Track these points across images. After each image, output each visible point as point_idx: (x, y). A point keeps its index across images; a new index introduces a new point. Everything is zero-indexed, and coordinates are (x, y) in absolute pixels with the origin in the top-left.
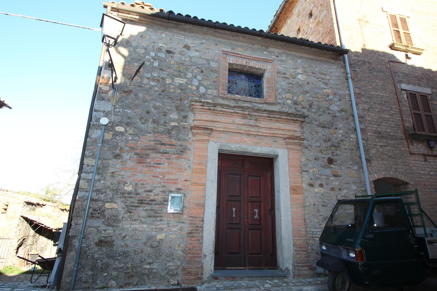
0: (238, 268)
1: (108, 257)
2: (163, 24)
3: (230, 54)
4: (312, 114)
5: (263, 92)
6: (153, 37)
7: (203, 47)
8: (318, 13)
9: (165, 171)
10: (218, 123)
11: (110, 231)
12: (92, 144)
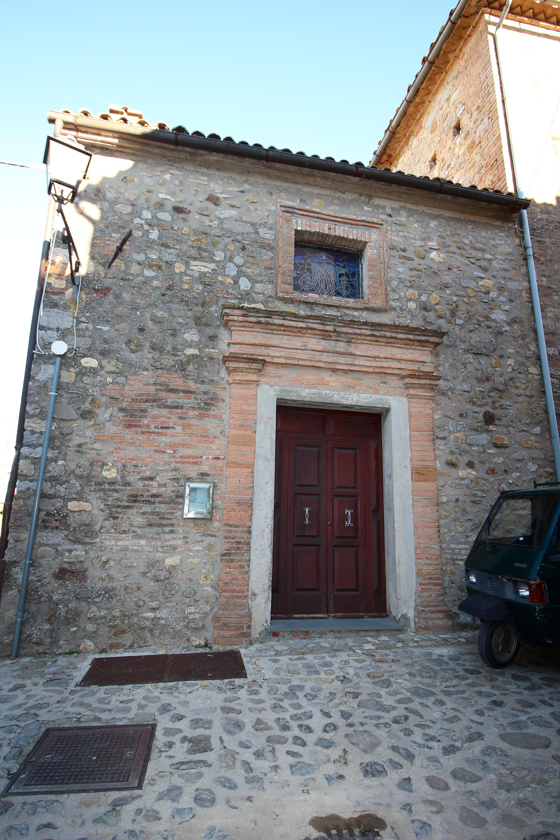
0: (315, 615)
1: (77, 598)
2: (167, 153)
3: (298, 212)
4: (457, 328)
5: (362, 286)
6: (148, 180)
7: (245, 199)
8: (472, 126)
9: (177, 440)
10: (275, 349)
11: (78, 553)
12: (38, 393)
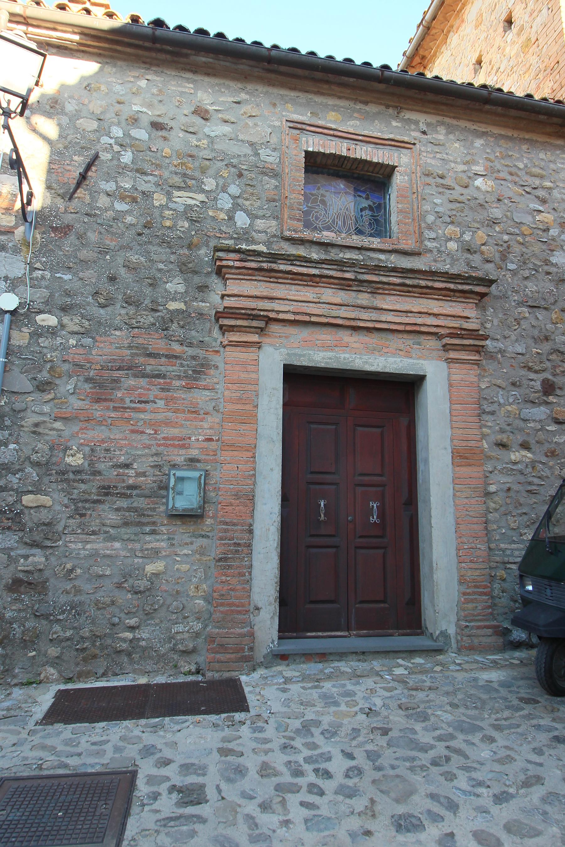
0: (333, 634)
4: (509, 275)
5: (390, 223)
6: (118, 88)
7: (242, 112)
9: (160, 417)
10: (281, 302)
11: (36, 559)
